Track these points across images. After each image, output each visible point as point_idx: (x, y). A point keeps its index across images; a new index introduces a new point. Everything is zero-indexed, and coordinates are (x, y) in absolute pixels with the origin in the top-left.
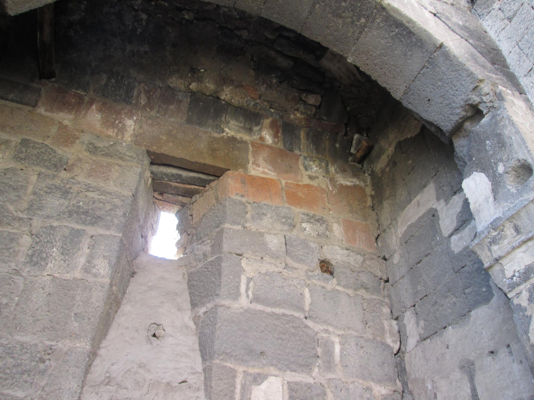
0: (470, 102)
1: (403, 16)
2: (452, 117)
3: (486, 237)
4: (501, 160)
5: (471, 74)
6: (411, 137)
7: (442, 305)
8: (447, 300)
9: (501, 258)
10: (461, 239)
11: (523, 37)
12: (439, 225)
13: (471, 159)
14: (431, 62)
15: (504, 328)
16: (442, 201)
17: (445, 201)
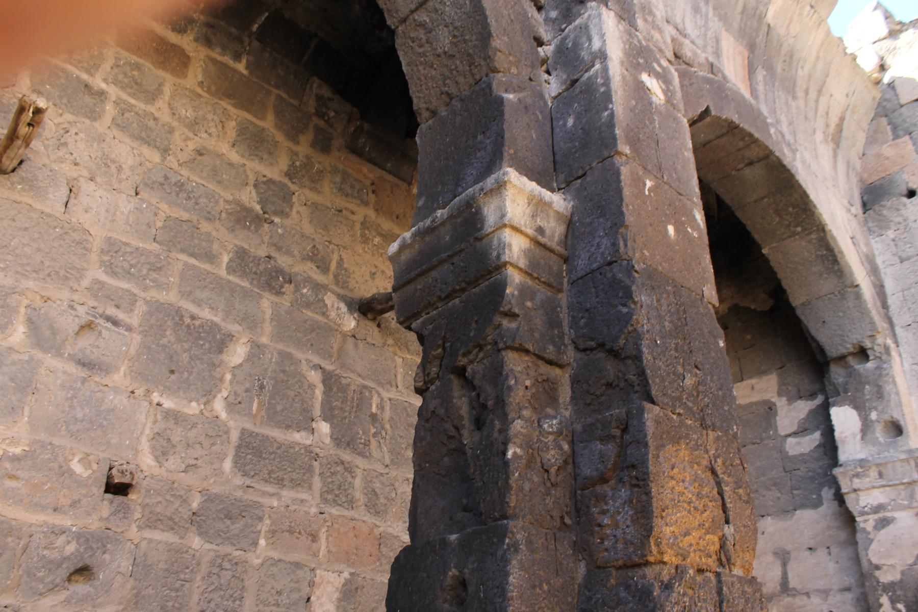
0: (863, 345)
1: (838, 245)
2: (840, 348)
3: (852, 470)
4: (876, 408)
5: (872, 323)
6: (755, 310)
7: (764, 496)
8: (770, 493)
9: (859, 490)
10: (799, 443)
11: (910, 289)
12: (776, 421)
13: (846, 392)
14: (843, 296)
15: (827, 533)
16: (784, 399)
17: (788, 400)
